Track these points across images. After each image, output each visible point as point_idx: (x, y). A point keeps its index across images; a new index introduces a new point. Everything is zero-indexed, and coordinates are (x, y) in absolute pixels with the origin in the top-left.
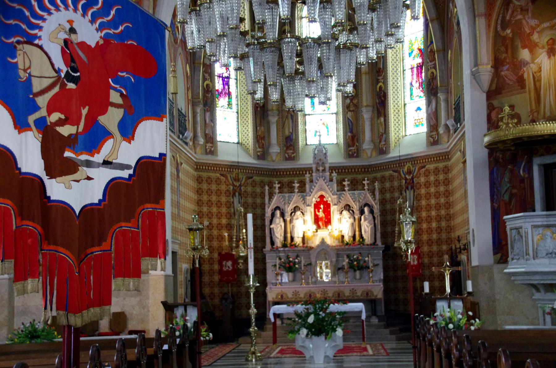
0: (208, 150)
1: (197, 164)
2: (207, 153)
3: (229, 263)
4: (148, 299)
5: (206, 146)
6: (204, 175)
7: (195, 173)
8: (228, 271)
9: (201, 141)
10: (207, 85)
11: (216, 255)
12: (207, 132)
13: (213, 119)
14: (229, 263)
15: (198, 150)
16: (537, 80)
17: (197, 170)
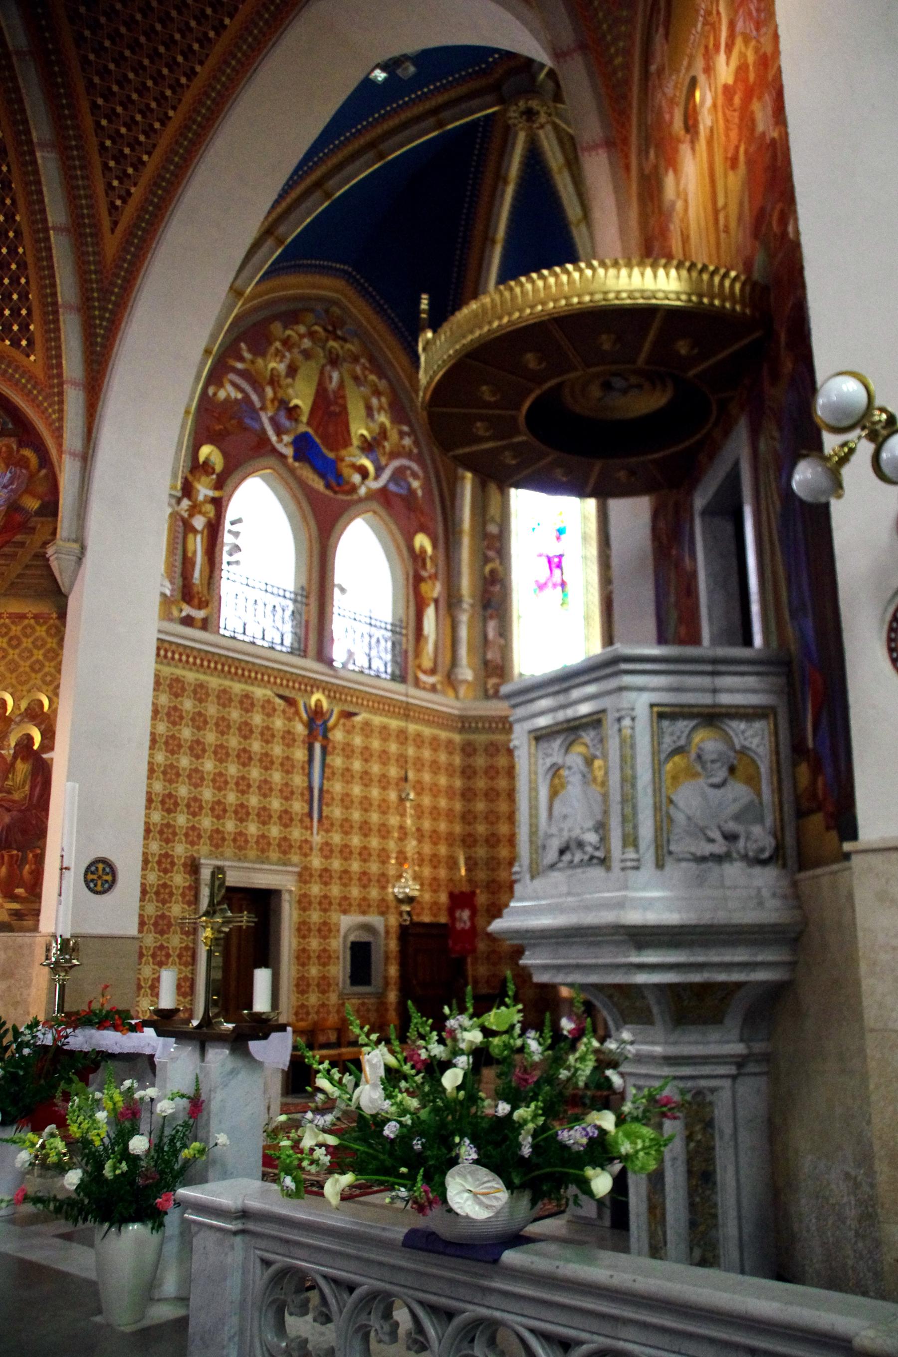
0: (491, 692)
1: (463, 719)
2: (487, 696)
3: (466, 914)
4: (28, 986)
5: (486, 683)
6: (481, 739)
7: (457, 738)
8: (463, 930)
9: (466, 673)
10: (492, 572)
11: (443, 898)
12: (489, 656)
13: (505, 631)
14: (466, 914)
15: (462, 691)
16: (686, 195)
17: (462, 730)
